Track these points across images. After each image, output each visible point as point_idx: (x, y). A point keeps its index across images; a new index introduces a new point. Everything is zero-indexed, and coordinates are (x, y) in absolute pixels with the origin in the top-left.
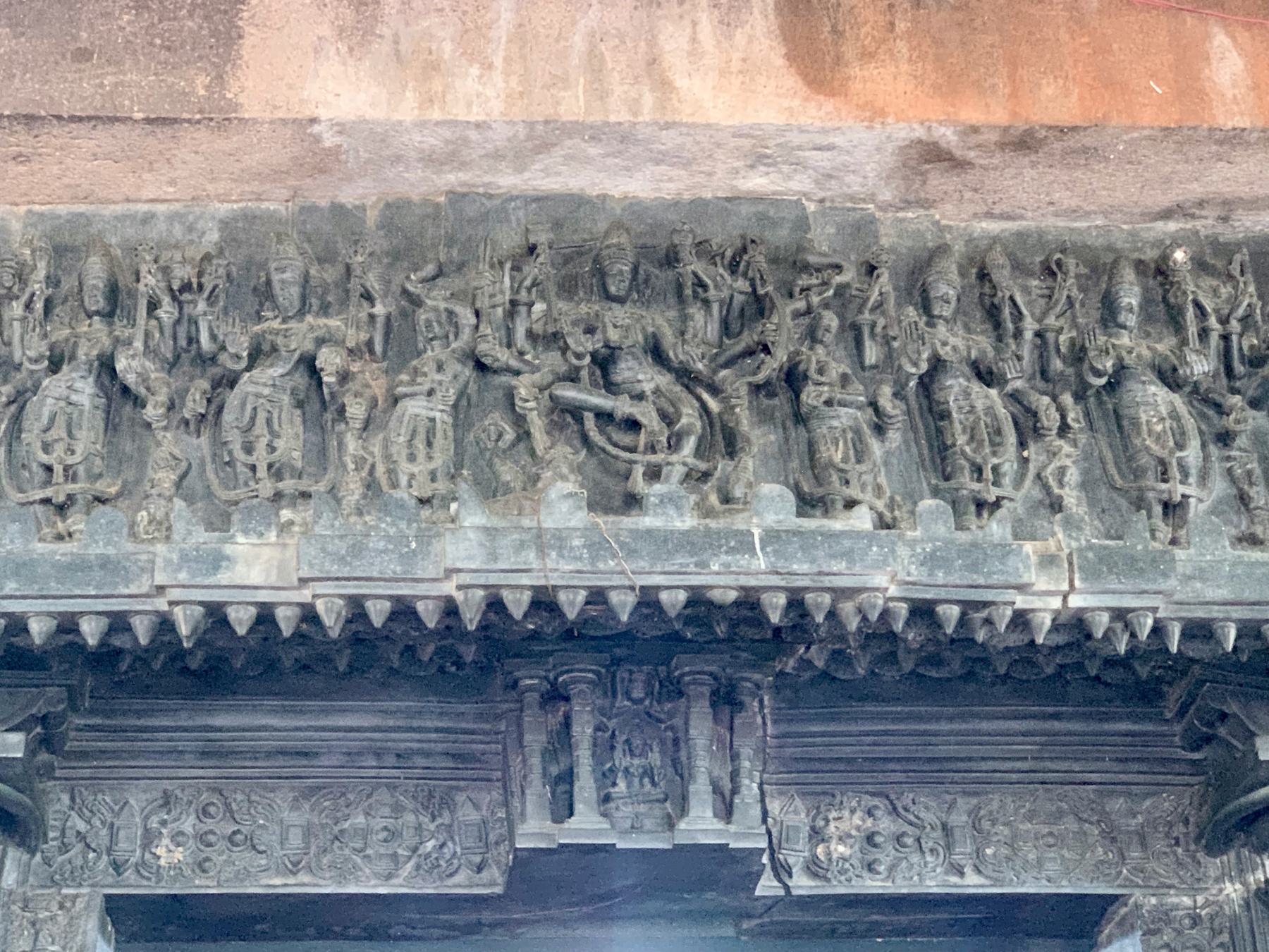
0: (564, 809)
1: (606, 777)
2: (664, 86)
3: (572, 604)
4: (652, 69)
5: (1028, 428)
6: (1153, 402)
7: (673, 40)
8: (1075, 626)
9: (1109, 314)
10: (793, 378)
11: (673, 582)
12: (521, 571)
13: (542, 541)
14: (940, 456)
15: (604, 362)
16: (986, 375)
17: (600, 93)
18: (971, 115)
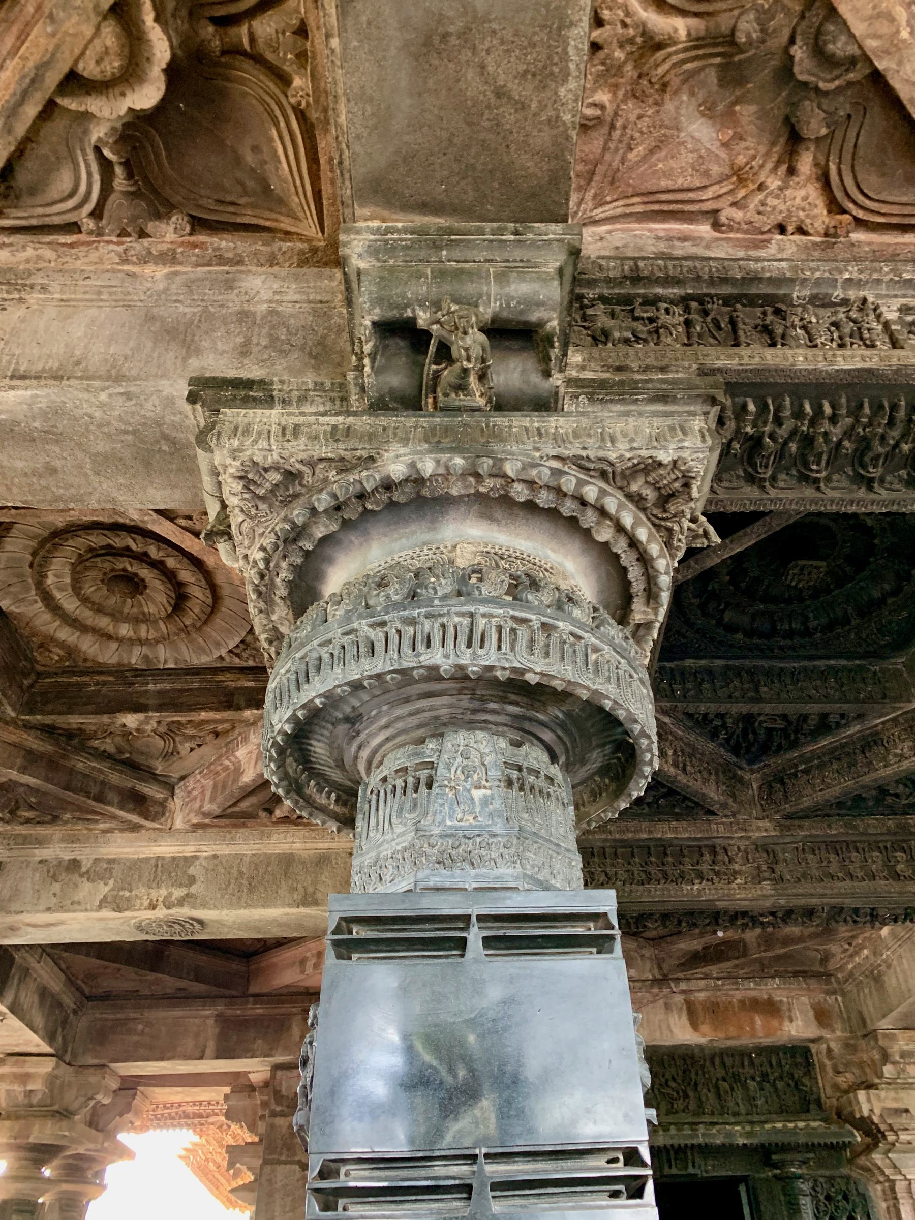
0: (670, 1167)
1: (676, 1159)
2: (671, 1031)
3: (676, 1146)
4: (669, 1027)
5: (732, 1089)
6: (752, 1084)
7: (671, 1021)
8: (745, 1145)
9: (743, 1065)
10: (696, 1084)
11: (689, 1142)
12: (669, 1142)
13: (672, 1137)
14: (719, 1096)
15: (667, 1081)
16: (724, 1080)
17: (662, 1034)
18: (720, 1035)
